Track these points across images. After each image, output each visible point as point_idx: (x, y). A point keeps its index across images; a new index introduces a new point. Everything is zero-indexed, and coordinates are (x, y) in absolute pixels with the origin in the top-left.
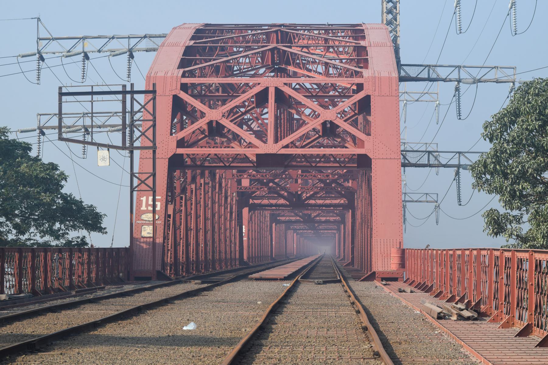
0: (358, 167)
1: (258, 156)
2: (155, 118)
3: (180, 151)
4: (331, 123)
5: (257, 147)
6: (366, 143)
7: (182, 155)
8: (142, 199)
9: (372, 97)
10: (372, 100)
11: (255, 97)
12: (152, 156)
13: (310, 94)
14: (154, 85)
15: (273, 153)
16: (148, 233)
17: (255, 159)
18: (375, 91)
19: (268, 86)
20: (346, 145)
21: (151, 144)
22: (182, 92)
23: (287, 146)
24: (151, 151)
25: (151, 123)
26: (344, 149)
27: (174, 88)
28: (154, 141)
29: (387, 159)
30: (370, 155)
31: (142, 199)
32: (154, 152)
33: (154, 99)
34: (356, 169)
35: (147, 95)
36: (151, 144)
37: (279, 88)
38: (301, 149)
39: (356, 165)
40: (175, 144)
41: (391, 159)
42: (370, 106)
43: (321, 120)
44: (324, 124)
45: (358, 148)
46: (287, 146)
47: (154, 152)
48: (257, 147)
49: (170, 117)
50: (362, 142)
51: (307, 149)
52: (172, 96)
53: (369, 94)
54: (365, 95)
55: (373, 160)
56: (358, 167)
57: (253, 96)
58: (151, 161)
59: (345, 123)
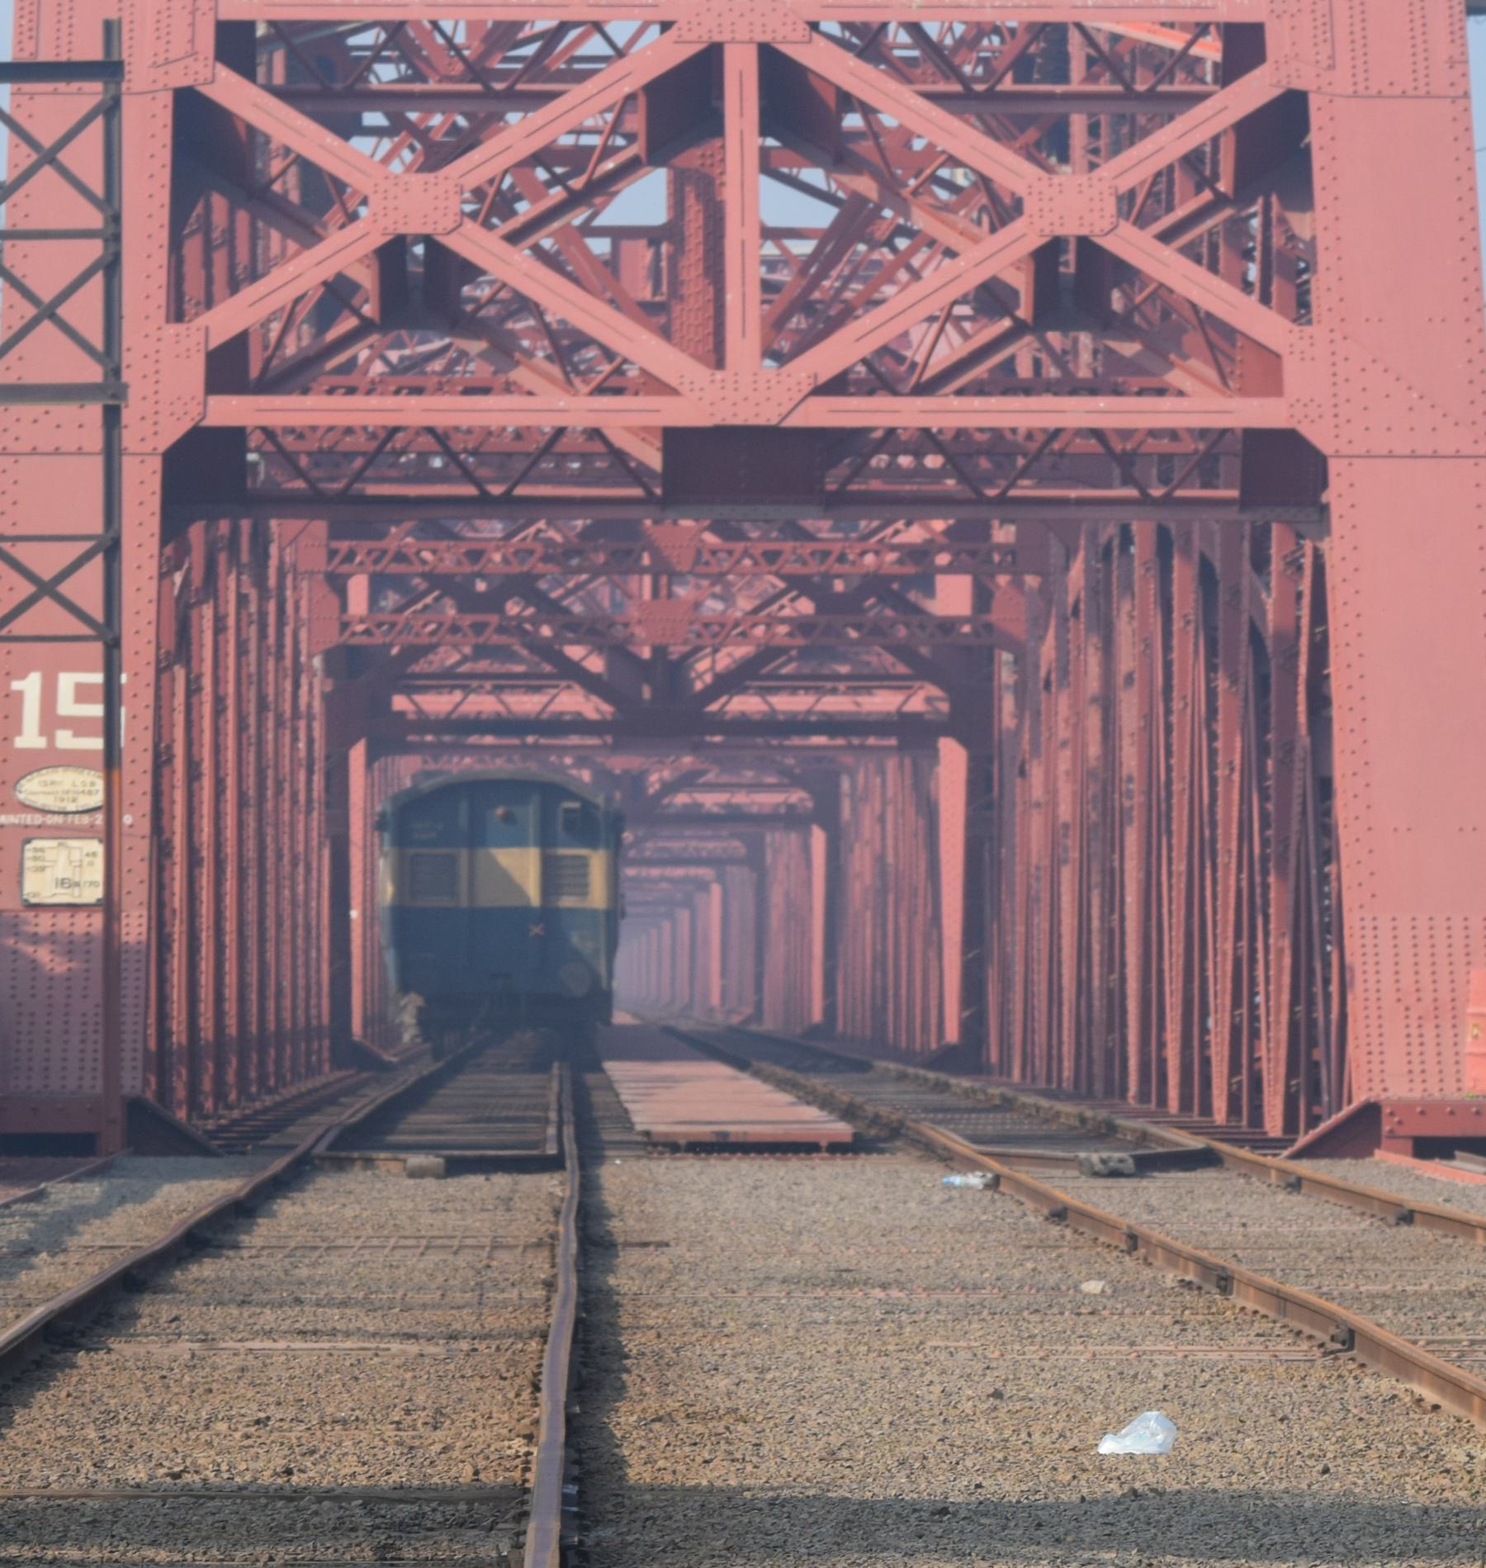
0: (1244, 503)
1: (675, 439)
2: (116, 219)
3: (229, 411)
4: (1084, 243)
5: (674, 392)
6: (1292, 371)
7: (235, 437)
8: (16, 685)
9: (1314, 102)
10: (1316, 118)
11: (642, 101)
12: (95, 439)
13: (957, 88)
14: (110, 30)
15: (761, 421)
16: (62, 882)
17: (653, 459)
18: (1332, 67)
19: (717, 38)
20: (1175, 377)
21: (93, 373)
22: (223, 72)
23: (838, 386)
24: (93, 412)
25: (94, 249)
26: (1167, 403)
27: (179, 48)
28: (110, 354)
29: (1413, 456)
30: (1319, 436)
31: (16, 685)
32: (112, 417)
33: (111, 110)
34: (1233, 514)
35: (27, 87)
36: (93, 373)
37: (786, 49)
38: (920, 402)
39: (1234, 493)
40: (196, 371)
41: (1434, 455)
42: (1306, 153)
43: (1025, 236)
44: (1047, 256)
45: (1243, 392)
46: (838, 386)
47: (112, 417)
48: (674, 392)
49: (164, 216)
50: (1270, 361)
51: (956, 402)
52: (167, 99)
53: (1297, 85)
54: (1277, 92)
55: (1334, 466)
56: (1244, 503)
57: (631, 98)
58: (98, 463)
59: (1168, 253)
